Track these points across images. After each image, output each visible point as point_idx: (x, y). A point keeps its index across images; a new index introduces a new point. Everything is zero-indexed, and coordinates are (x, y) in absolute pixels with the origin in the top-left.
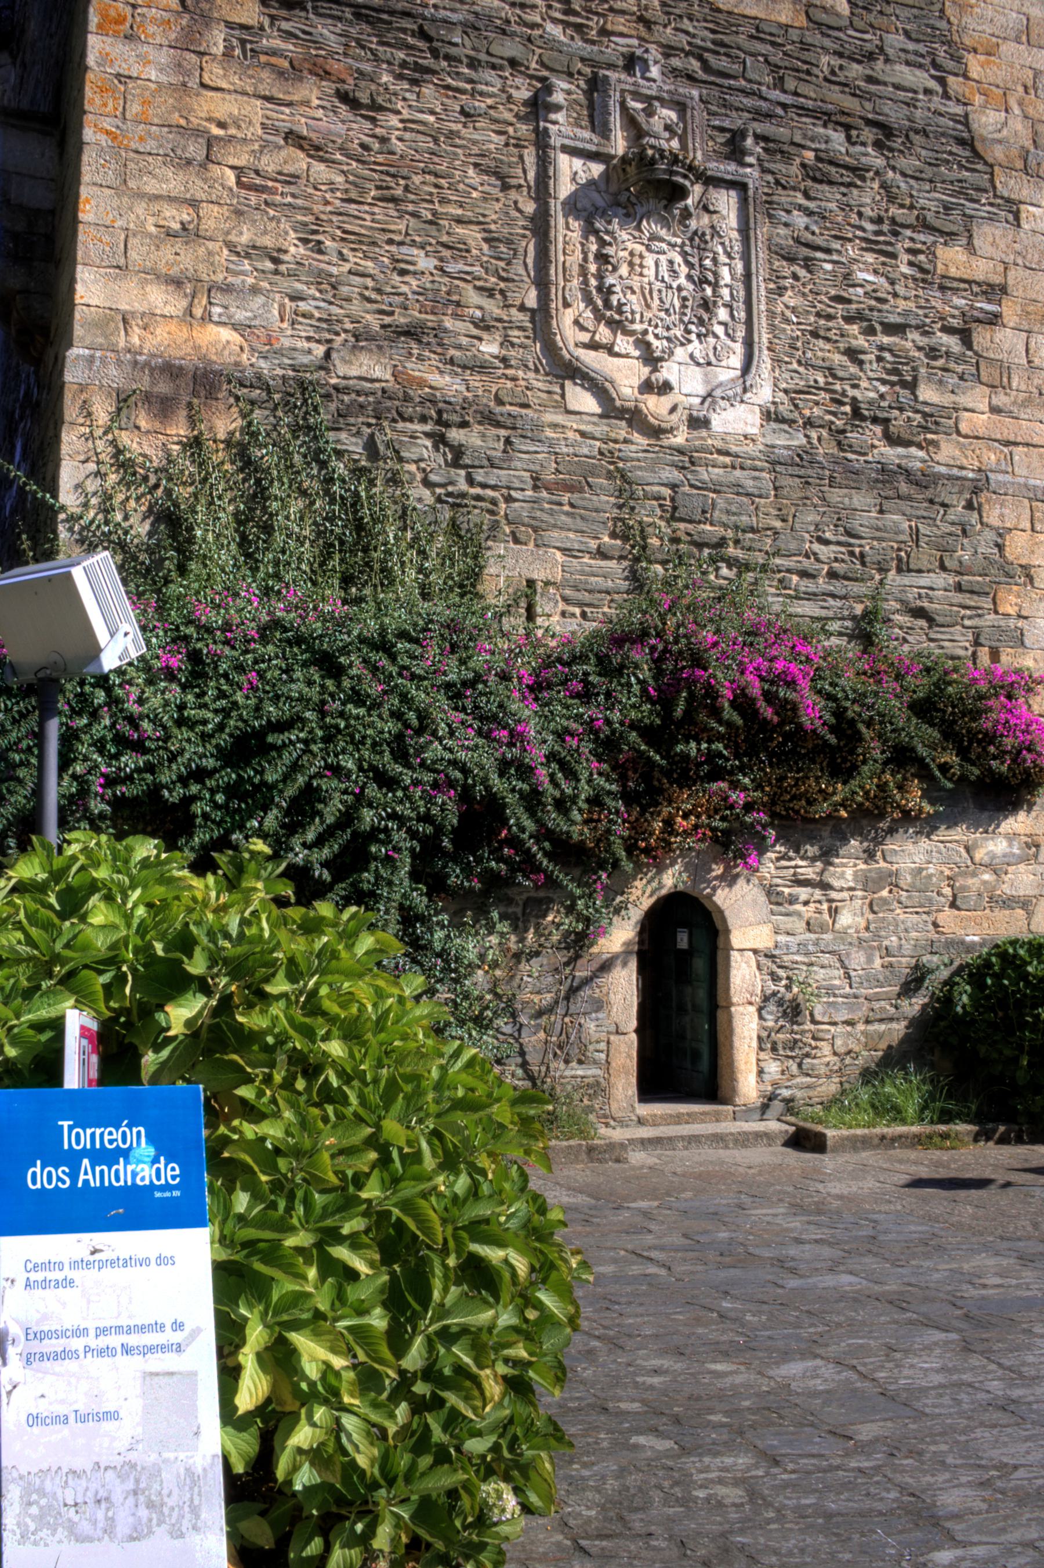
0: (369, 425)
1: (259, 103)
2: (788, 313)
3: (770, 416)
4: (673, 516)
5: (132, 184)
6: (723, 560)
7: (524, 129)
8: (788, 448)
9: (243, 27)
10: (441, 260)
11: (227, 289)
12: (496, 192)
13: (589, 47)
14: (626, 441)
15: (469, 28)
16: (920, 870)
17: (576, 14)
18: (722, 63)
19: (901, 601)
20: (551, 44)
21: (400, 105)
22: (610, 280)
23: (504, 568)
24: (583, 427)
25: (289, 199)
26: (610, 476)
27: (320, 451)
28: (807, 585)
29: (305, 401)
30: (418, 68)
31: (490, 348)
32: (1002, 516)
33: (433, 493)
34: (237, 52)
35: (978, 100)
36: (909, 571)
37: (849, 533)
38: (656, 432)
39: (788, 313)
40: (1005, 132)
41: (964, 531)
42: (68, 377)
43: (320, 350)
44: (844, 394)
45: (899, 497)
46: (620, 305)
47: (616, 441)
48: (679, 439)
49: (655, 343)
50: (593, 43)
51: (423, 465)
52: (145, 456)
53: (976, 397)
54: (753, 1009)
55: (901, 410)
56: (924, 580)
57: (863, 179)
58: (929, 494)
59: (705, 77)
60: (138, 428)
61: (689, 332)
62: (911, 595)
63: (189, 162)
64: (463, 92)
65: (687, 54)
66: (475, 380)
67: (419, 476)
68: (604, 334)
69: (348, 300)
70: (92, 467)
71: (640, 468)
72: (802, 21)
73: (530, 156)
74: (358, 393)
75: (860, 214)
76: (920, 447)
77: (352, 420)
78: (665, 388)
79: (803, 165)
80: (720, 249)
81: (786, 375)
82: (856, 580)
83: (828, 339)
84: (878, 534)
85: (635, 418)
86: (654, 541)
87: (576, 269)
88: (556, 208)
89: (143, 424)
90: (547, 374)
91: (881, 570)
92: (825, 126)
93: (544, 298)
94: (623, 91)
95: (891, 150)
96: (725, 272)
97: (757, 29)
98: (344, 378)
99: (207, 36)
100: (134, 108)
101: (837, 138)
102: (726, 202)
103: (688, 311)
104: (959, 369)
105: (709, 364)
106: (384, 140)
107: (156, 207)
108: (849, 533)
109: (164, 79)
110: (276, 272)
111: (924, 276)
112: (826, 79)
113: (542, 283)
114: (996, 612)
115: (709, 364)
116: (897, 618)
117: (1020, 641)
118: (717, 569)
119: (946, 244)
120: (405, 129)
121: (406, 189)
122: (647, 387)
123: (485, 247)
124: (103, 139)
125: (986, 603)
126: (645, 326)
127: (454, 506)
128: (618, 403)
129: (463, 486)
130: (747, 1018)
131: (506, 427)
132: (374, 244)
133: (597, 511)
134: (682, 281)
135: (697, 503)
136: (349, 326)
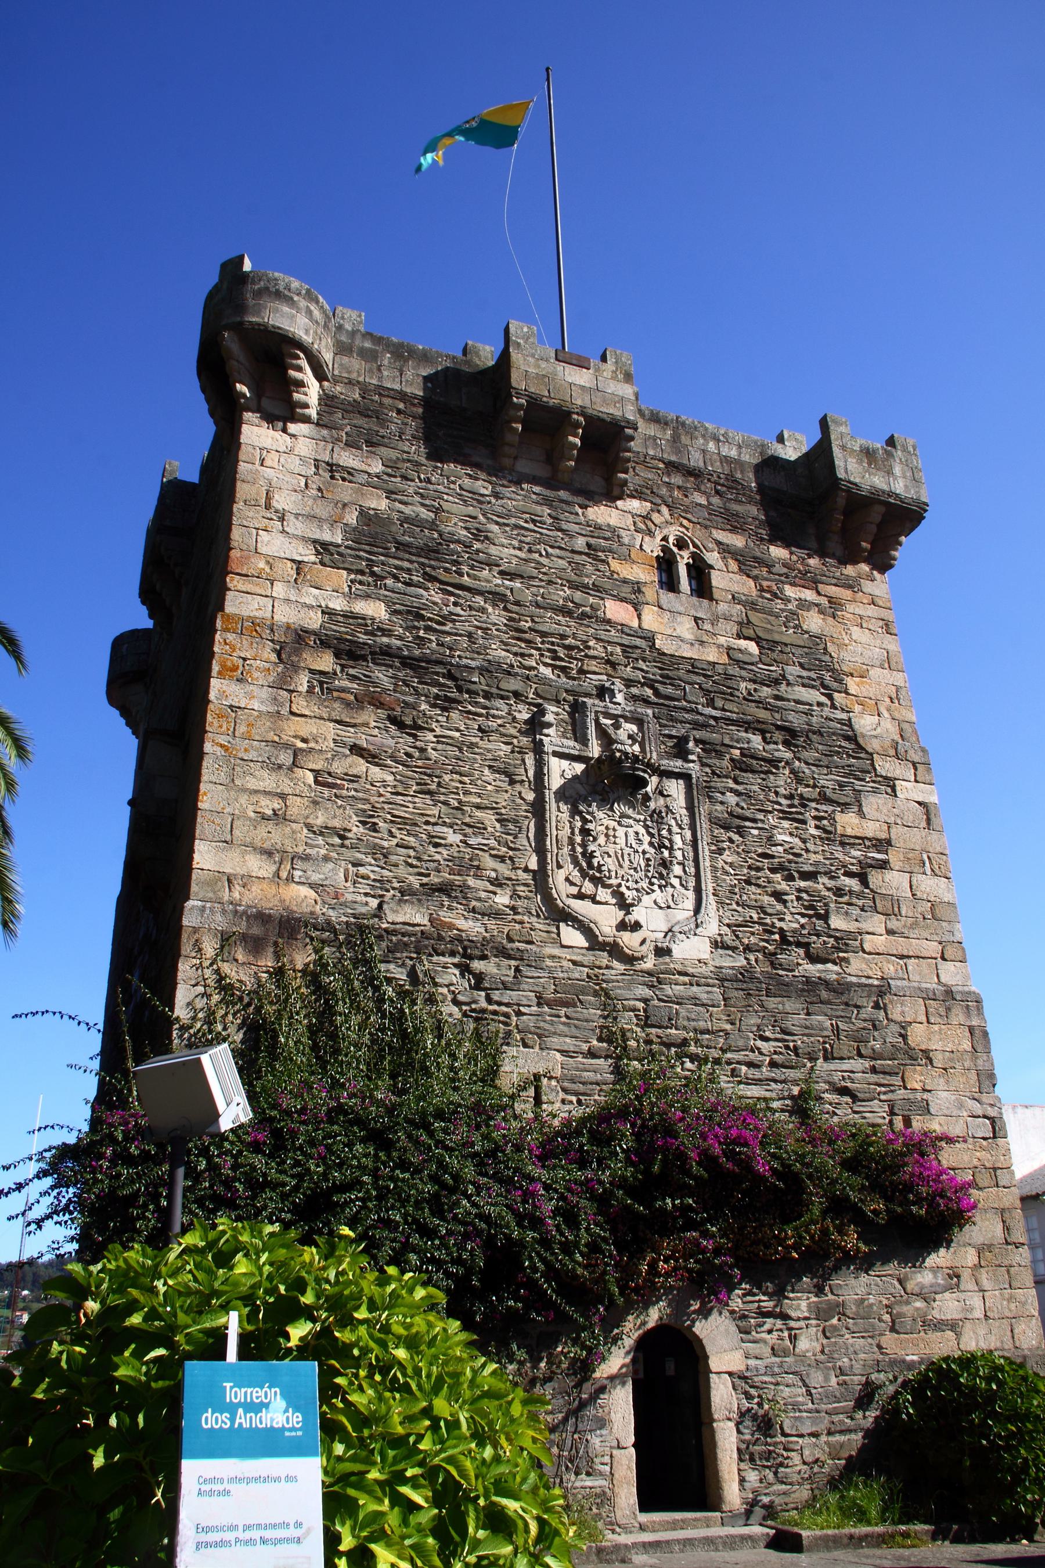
0: (411, 959)
1: (332, 724)
2: (727, 867)
3: (717, 944)
4: (646, 1022)
5: (238, 782)
6: (687, 1056)
7: (525, 740)
8: (733, 968)
9: (322, 673)
10: (465, 835)
11: (306, 858)
12: (505, 786)
13: (571, 682)
14: (608, 967)
15: (482, 671)
16: (862, 1300)
17: (561, 659)
18: (669, 690)
19: (829, 1083)
20: (543, 681)
21: (434, 725)
22: (591, 848)
23: (517, 1064)
24: (574, 958)
25: (353, 793)
26: (596, 994)
27: (373, 978)
28: (752, 1073)
29: (363, 941)
30: (447, 699)
31: (502, 899)
32: (903, 1013)
33: (461, 1010)
34: (317, 689)
35: (857, 708)
36: (834, 1058)
37: (784, 1031)
38: (630, 960)
39: (727, 867)
40: (879, 730)
41: (874, 1026)
42: (185, 922)
43: (374, 903)
44: (773, 925)
45: (821, 1002)
46: (600, 866)
47: (600, 968)
48: (649, 964)
49: (627, 893)
50: (574, 679)
51: (452, 988)
52: (240, 981)
53: (875, 923)
54: (731, 1424)
55: (818, 935)
56: (846, 1065)
57: (777, 768)
58: (844, 998)
59: (656, 700)
60: (236, 960)
61: (652, 884)
62: (837, 1077)
63: (280, 767)
64: (480, 715)
65: (643, 685)
66: (492, 924)
67: (450, 997)
68: (588, 887)
69: (396, 865)
70: (200, 989)
71: (619, 988)
72: (725, 659)
73: (530, 760)
74: (403, 935)
75: (776, 793)
76: (835, 963)
77: (398, 955)
78: (636, 926)
79: (732, 760)
80: (673, 822)
81: (729, 914)
82: (792, 1067)
83: (758, 886)
84: (807, 1031)
85: (615, 950)
86: (632, 1043)
87: (565, 841)
88: (550, 796)
89: (240, 957)
90: (546, 918)
91: (813, 1059)
92: (746, 731)
93: (542, 862)
94: (596, 712)
95: (796, 746)
96: (677, 839)
97: (693, 666)
98: (393, 923)
99: (296, 679)
100: (242, 729)
101: (756, 741)
102: (676, 789)
103: (651, 869)
104: (860, 903)
105: (669, 907)
106: (422, 750)
107: (254, 798)
108: (784, 1031)
109: (263, 708)
110: (343, 846)
111: (828, 836)
112: (745, 699)
113: (541, 851)
114: (905, 1088)
115: (669, 907)
116: (826, 1095)
117: (926, 1110)
118: (683, 1063)
119: (842, 812)
120: (438, 742)
121: (439, 784)
122: (622, 926)
123: (498, 825)
124: (219, 751)
125: (897, 1081)
126: (619, 881)
127: (477, 1020)
128: (601, 939)
129: (483, 1004)
130: (727, 1433)
131: (515, 959)
132: (416, 825)
133: (587, 1021)
134: (646, 846)
135: (664, 1013)
136: (396, 885)
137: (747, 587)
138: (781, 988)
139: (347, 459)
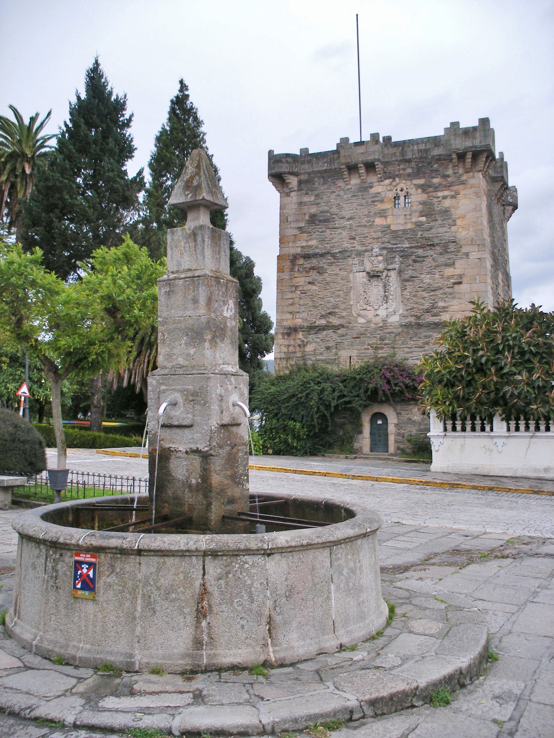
11: (299, 312)
53: (455, 302)
100: (284, 284)
101: (420, 252)
111: (442, 277)
137: (423, 197)
138: (419, 326)
139: (306, 199)
